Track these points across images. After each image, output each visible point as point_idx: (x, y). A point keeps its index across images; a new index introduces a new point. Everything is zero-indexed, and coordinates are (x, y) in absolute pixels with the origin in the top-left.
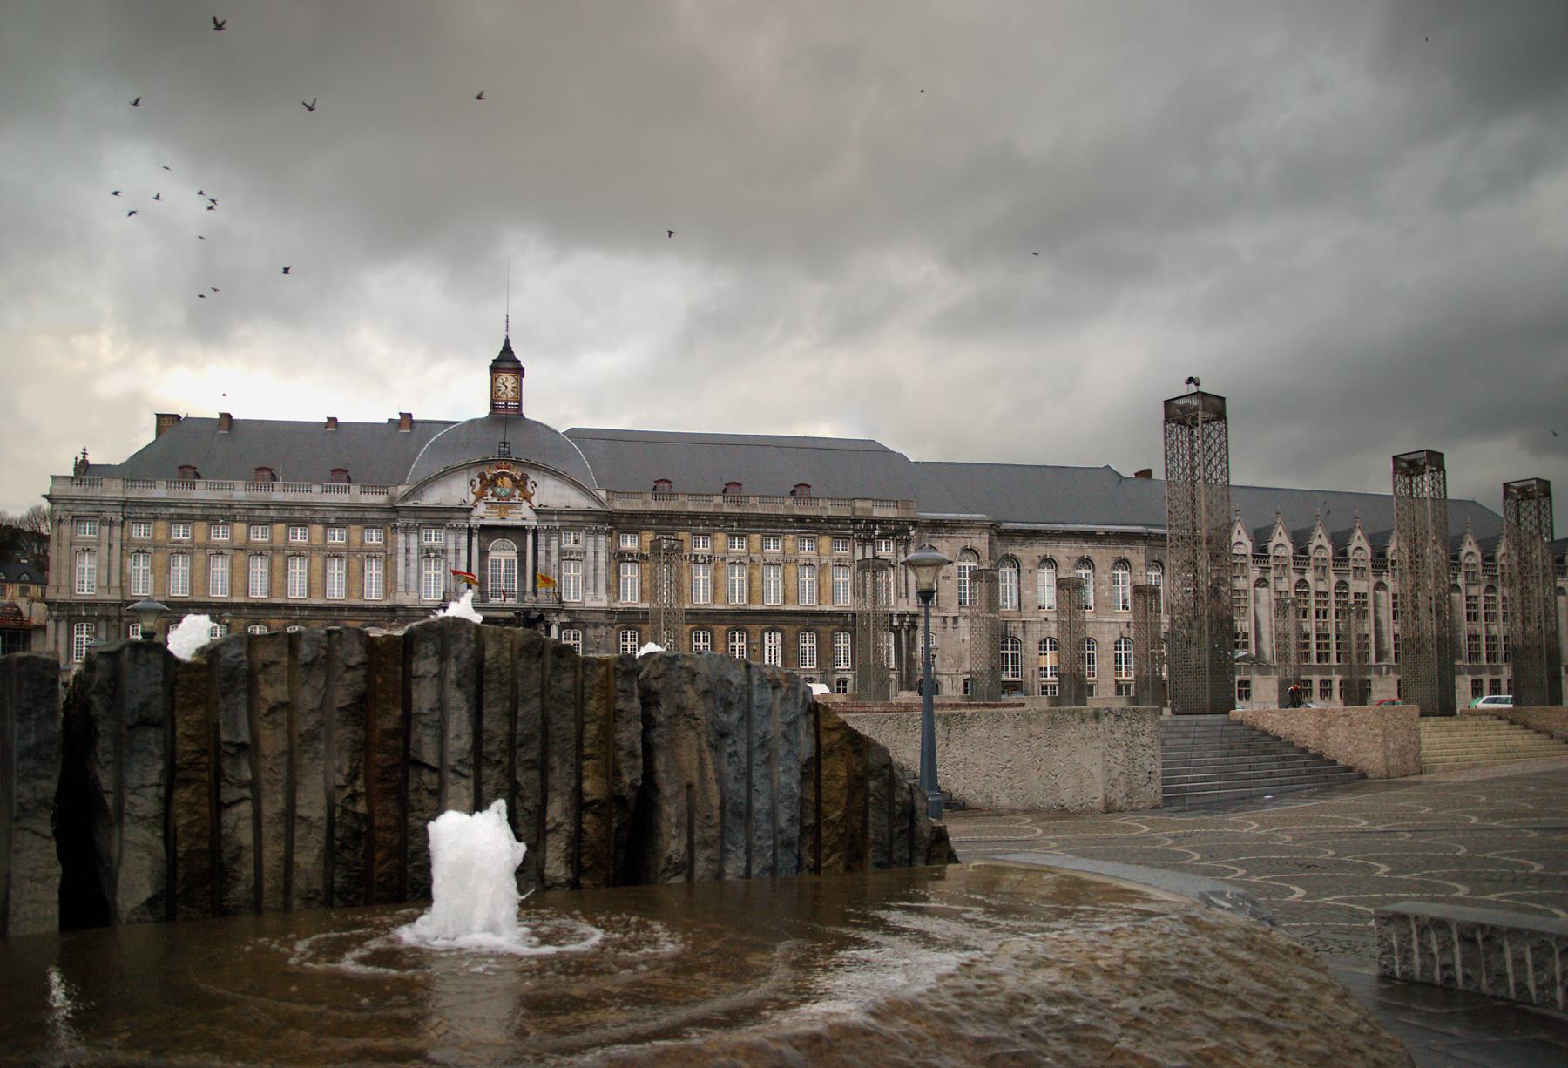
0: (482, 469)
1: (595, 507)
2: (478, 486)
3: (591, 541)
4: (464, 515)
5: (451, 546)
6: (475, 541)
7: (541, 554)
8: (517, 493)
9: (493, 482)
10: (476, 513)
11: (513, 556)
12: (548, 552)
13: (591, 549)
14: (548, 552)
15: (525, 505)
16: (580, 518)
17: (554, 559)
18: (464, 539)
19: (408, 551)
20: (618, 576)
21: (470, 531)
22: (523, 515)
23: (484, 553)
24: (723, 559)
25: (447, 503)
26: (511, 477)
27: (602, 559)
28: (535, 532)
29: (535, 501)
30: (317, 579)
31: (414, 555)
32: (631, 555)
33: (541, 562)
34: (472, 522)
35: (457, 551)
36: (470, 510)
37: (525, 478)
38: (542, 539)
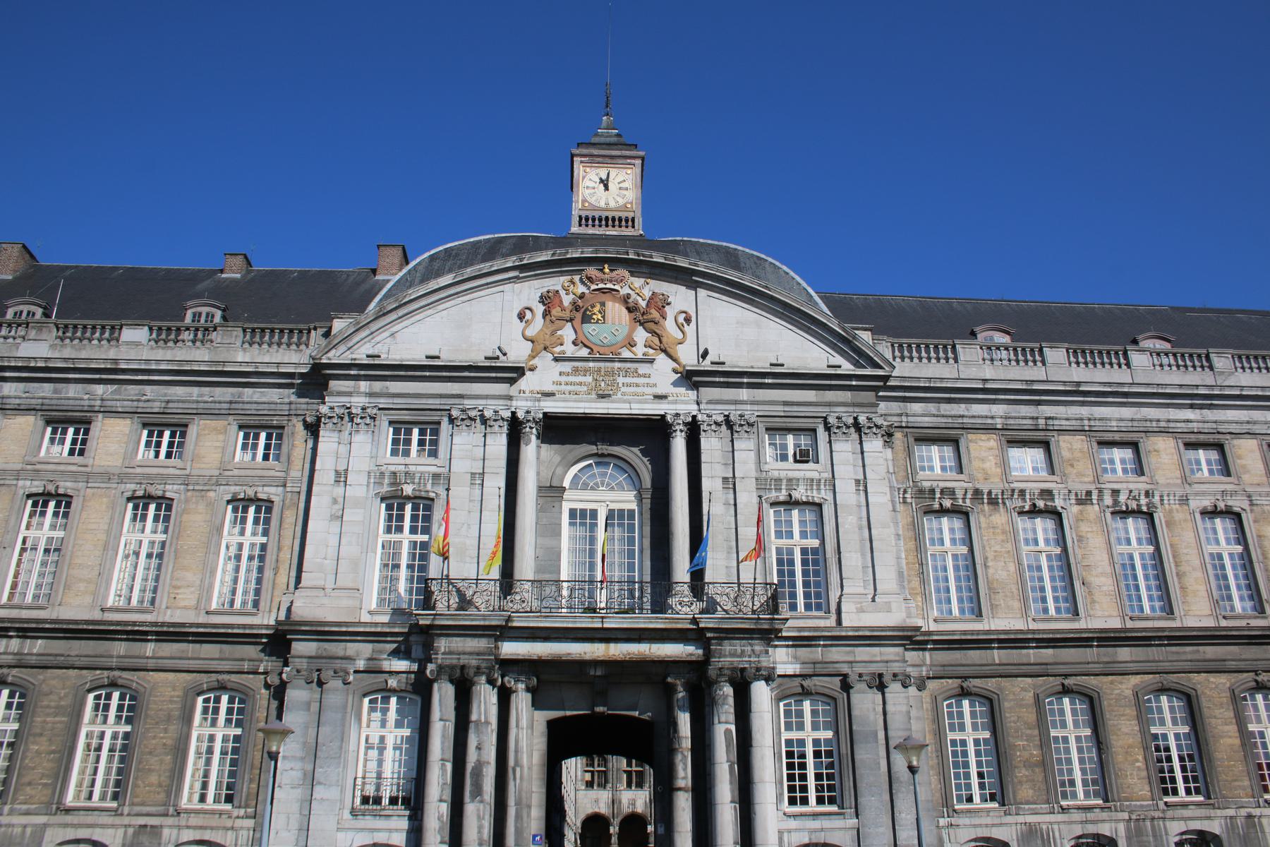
0: (555, 283)
1: (847, 367)
2: (539, 321)
3: (845, 448)
4: (500, 388)
5: (462, 467)
6: (531, 450)
7: (709, 484)
8: (641, 335)
9: (582, 313)
10: (528, 382)
11: (627, 500)
12: (730, 483)
13: (846, 472)
14: (730, 483)
15: (662, 362)
16: (810, 395)
17: (747, 497)
18: (499, 444)
19: (341, 477)
20: (920, 548)
21: (515, 429)
22: (649, 391)
23: (551, 492)
24: (1184, 500)
25: (449, 356)
26: (625, 300)
27: (880, 497)
28: (693, 431)
29: (688, 357)
30: (85, 554)
31: (359, 487)
32: (951, 492)
33: (715, 508)
34: (521, 407)
35: (479, 478)
36: (519, 371)
37: (659, 303)
38: (711, 445)
